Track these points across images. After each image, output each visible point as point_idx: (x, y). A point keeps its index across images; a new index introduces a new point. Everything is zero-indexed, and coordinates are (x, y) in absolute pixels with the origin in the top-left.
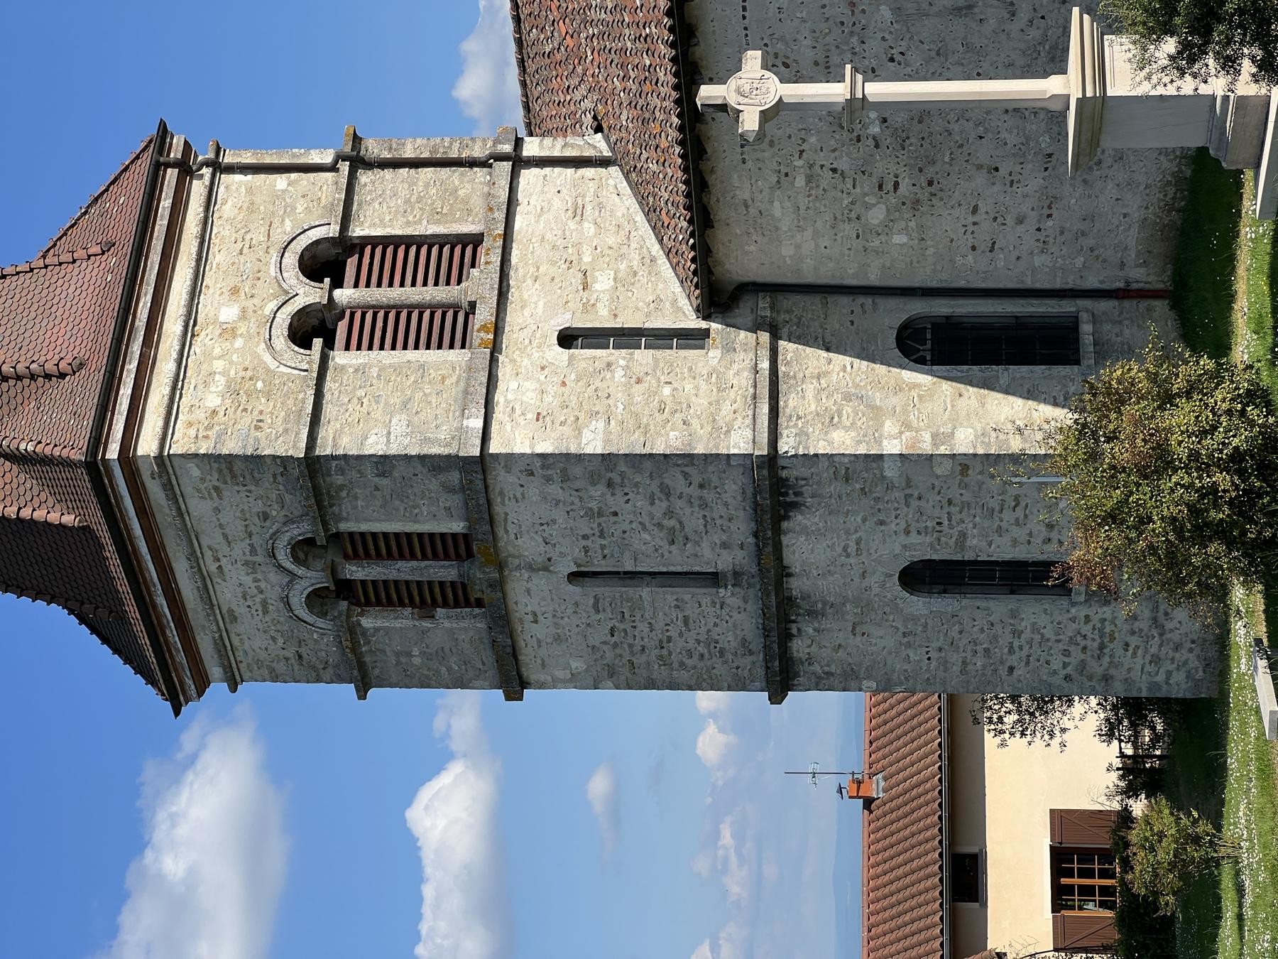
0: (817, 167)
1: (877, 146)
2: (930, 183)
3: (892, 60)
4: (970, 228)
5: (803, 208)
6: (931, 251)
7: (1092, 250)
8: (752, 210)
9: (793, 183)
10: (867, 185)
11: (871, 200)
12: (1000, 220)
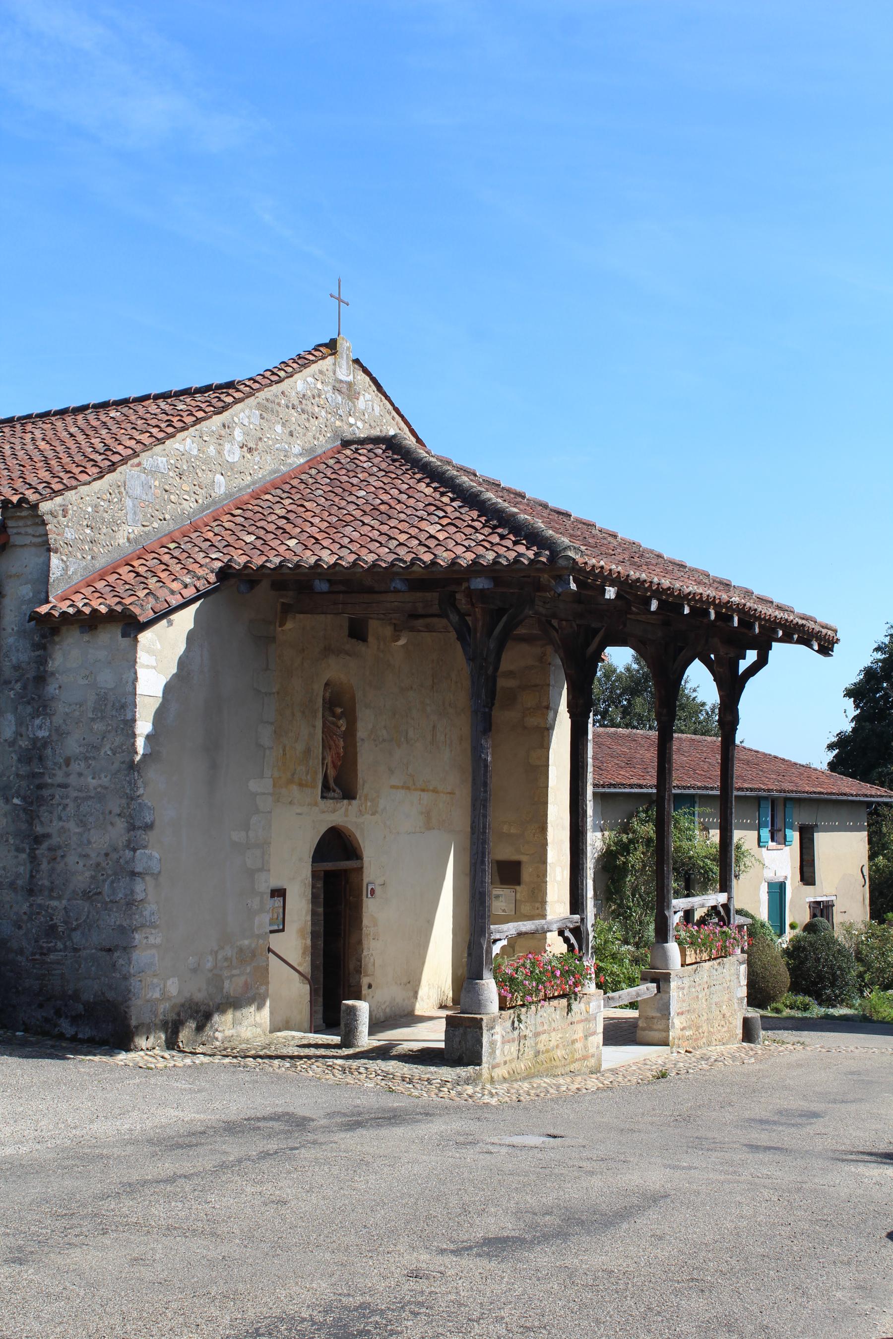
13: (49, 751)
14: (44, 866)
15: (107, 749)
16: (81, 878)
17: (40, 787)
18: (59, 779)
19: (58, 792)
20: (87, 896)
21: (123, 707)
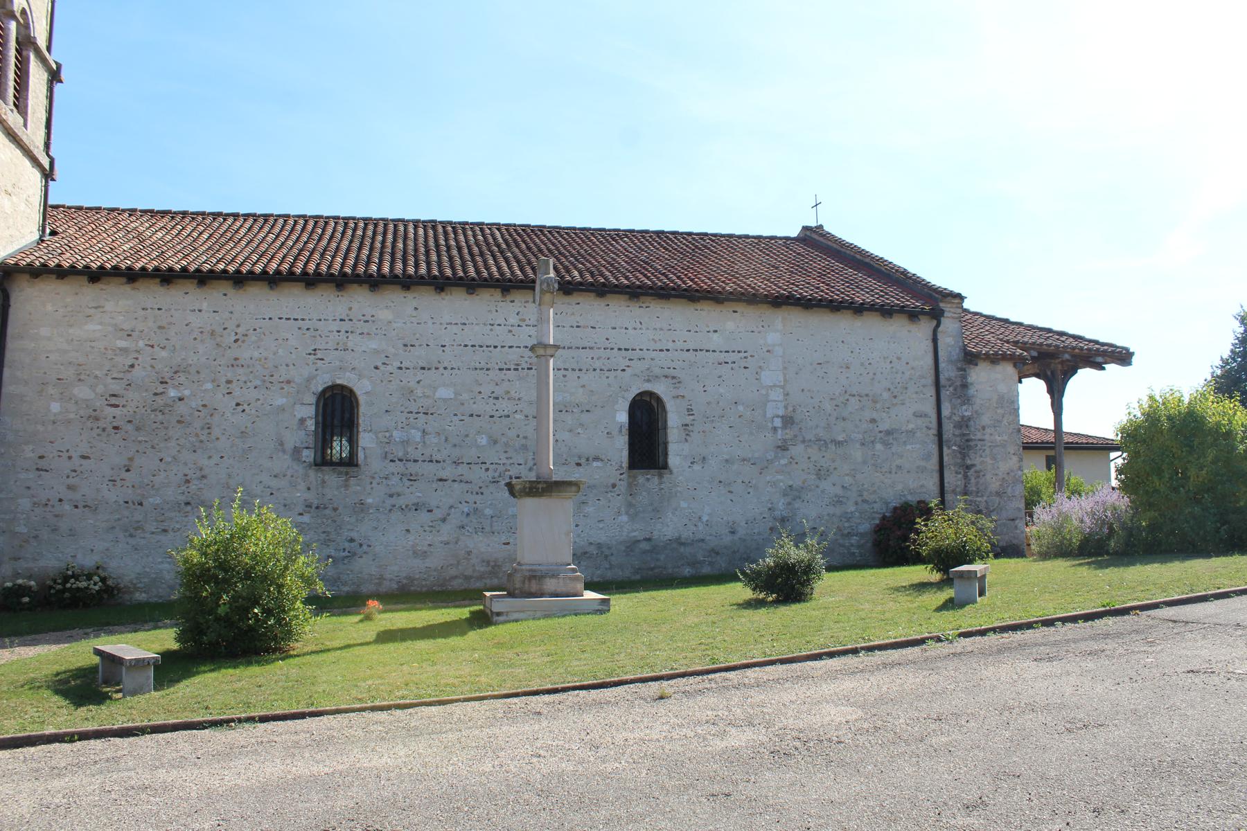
0: (136, 355)
1: (156, 394)
2: (116, 428)
3: (238, 404)
4: (65, 455)
5: (93, 344)
6: (40, 428)
7: (36, 537)
8: (93, 311)
9: (120, 338)
10: (116, 387)
11: (100, 389)
12: (74, 474)
13: (972, 423)
14: (973, 481)
15: (1005, 422)
16: (994, 486)
17: (968, 441)
18: (979, 436)
19: (979, 443)
20: (998, 494)
21: (1013, 402)
